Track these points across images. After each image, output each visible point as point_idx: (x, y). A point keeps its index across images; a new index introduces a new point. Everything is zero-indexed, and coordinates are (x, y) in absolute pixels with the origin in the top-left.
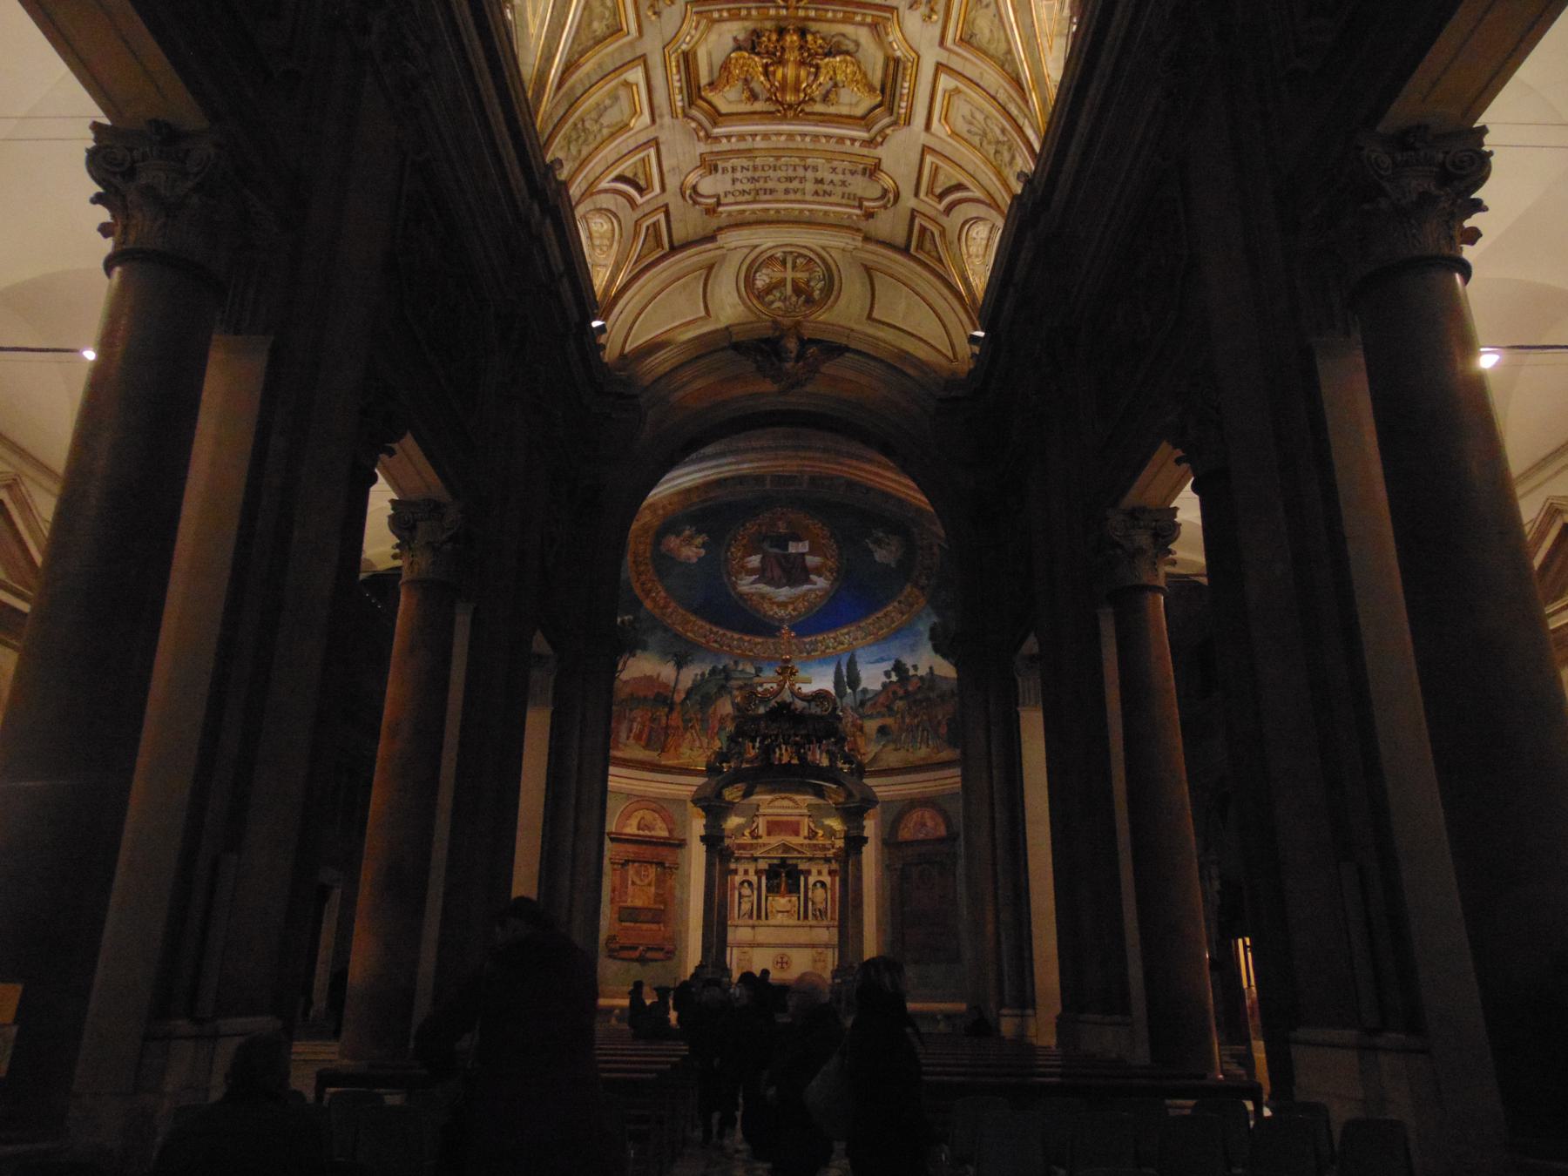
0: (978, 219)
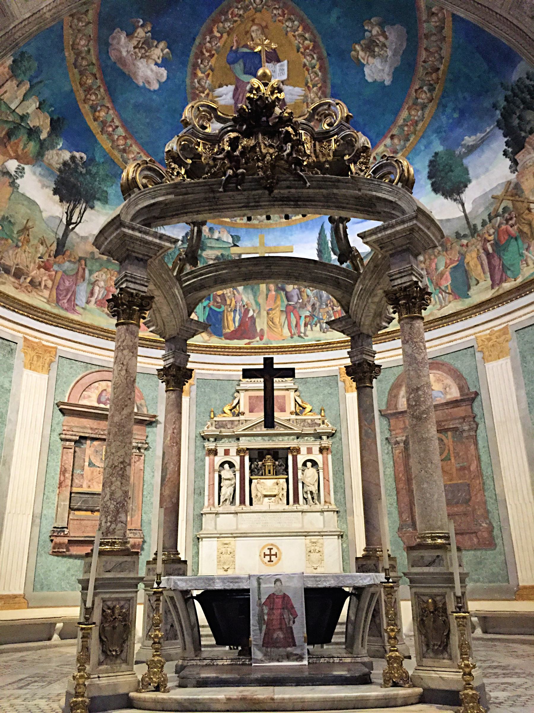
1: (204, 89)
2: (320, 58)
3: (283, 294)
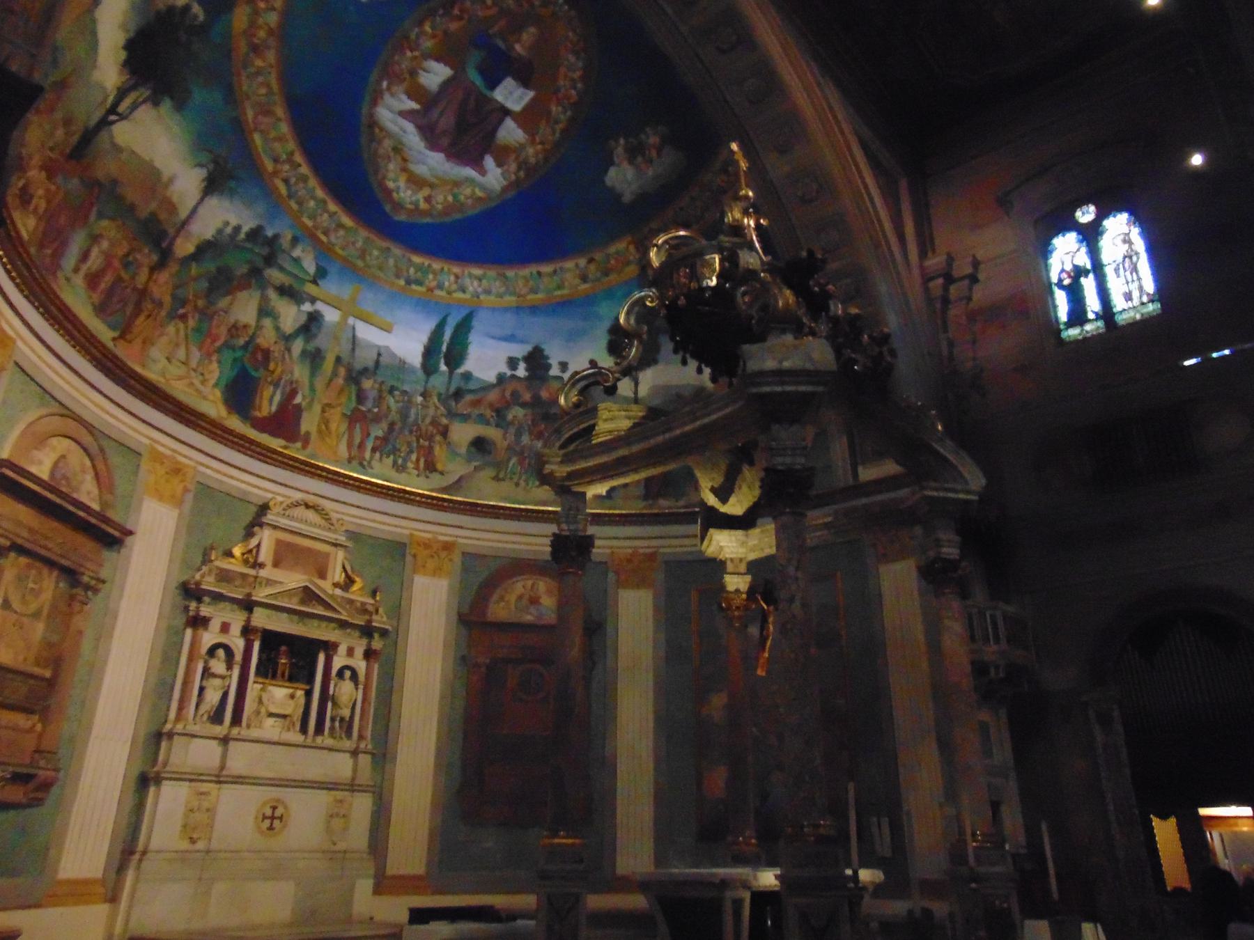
3: (353, 388)
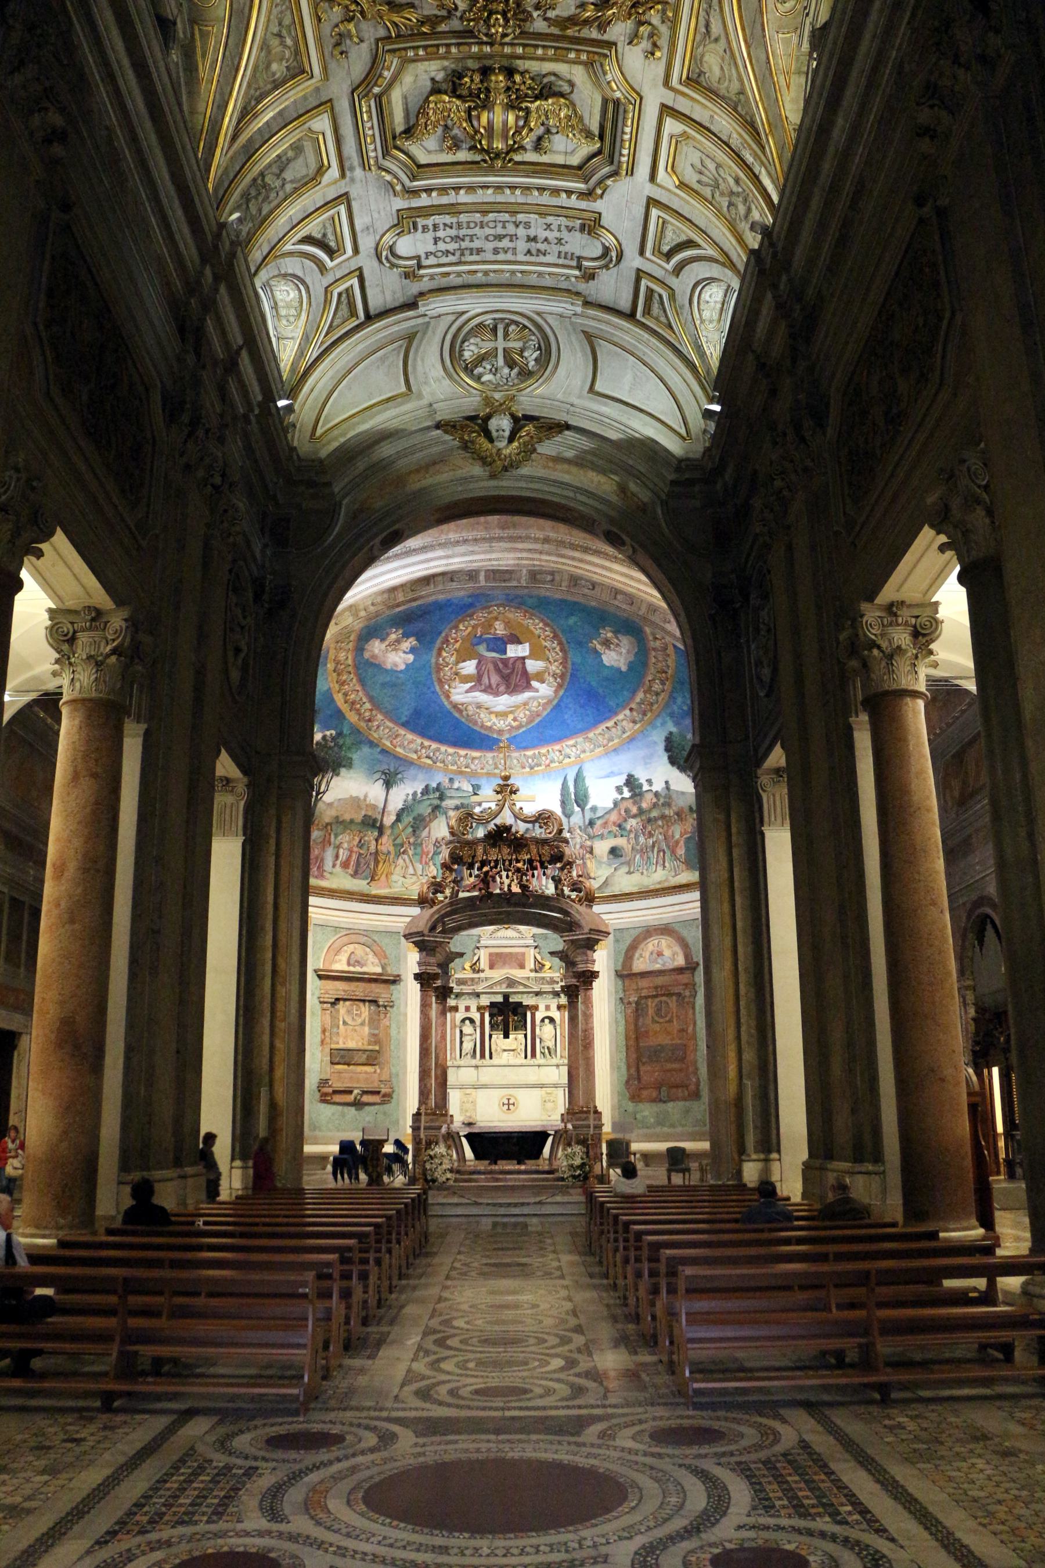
0: (712, 280)
1: (448, 664)
2: (560, 643)
